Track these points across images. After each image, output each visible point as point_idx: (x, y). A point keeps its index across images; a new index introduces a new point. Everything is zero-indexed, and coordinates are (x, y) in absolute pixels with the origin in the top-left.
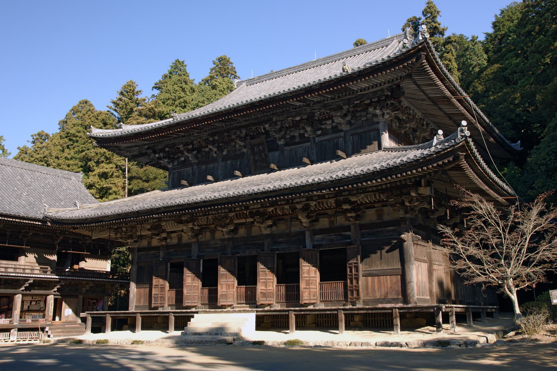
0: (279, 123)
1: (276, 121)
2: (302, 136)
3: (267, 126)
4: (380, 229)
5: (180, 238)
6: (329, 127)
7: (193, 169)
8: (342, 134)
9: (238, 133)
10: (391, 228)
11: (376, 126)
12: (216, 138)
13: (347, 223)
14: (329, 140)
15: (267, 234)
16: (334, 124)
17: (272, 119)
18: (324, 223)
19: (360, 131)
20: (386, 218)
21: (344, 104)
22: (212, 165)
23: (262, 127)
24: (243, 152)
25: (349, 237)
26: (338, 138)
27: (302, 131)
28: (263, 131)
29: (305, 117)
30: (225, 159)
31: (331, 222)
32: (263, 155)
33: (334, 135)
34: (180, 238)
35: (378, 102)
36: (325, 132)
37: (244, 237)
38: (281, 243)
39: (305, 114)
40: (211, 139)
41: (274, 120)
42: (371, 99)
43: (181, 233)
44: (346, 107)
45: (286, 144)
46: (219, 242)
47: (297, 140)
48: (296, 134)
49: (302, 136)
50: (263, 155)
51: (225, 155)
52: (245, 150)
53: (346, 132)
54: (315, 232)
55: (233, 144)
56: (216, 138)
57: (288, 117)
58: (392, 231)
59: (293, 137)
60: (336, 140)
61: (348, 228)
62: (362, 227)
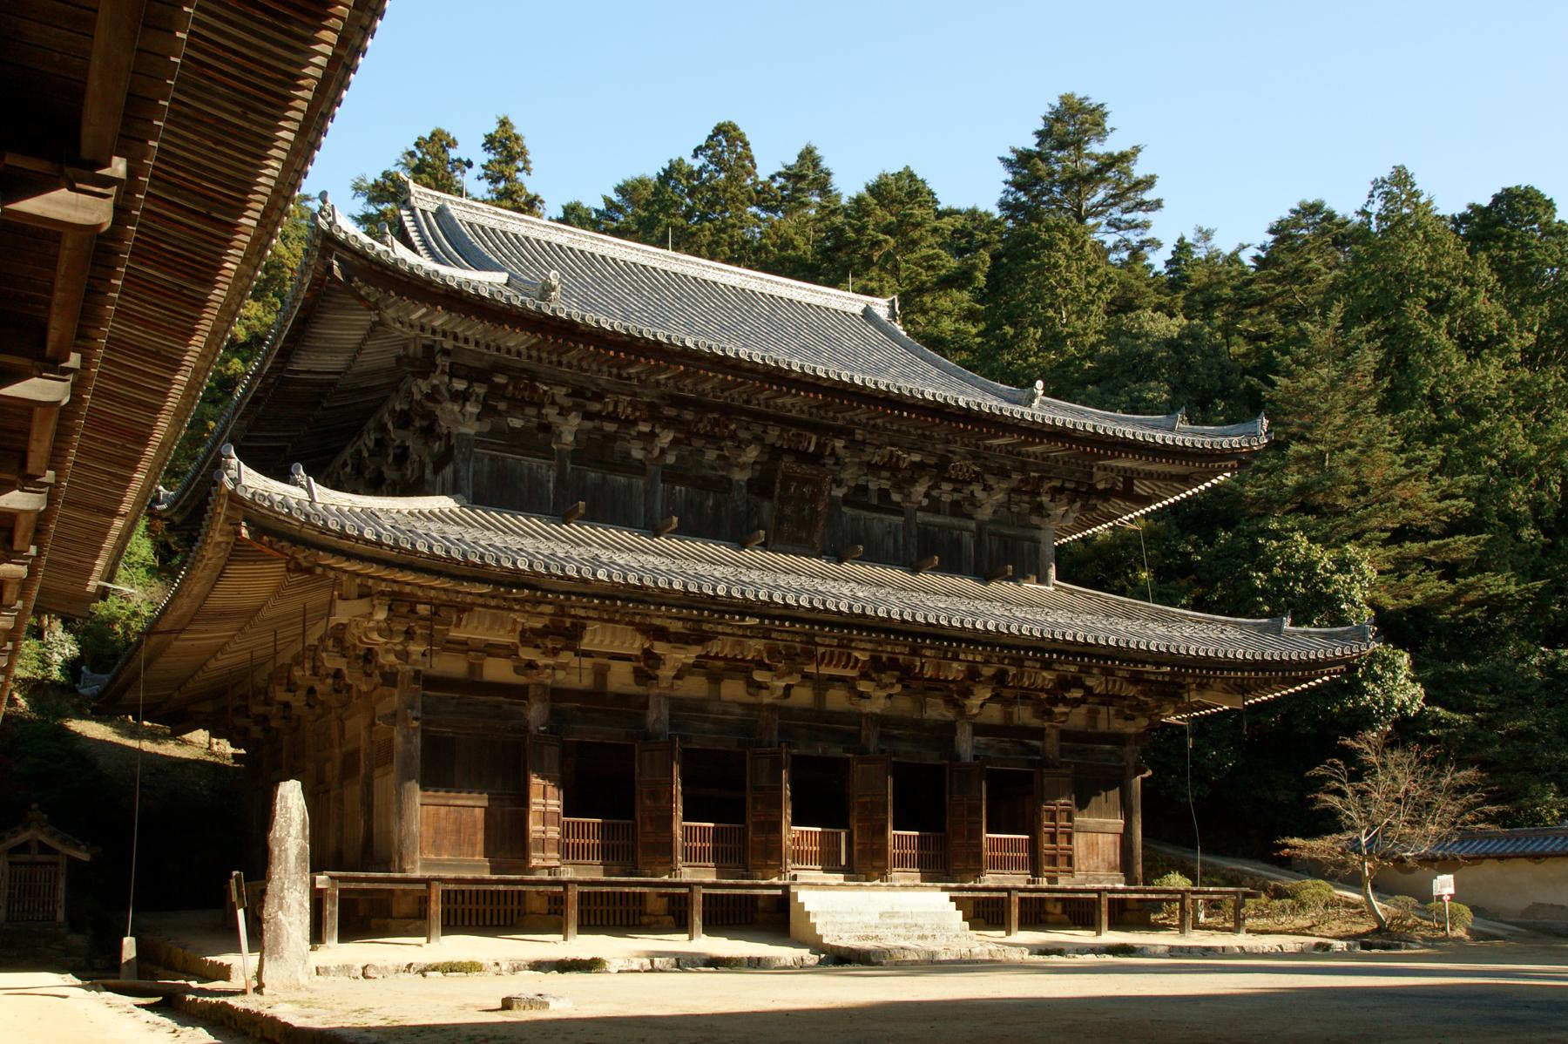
0: (869, 449)
1: (864, 442)
2: (884, 494)
3: (839, 444)
4: (1089, 746)
5: (601, 674)
6: (946, 498)
7: (561, 471)
8: (973, 525)
9: (757, 429)
10: (1108, 747)
11: (1036, 533)
12: (689, 415)
13: (1035, 722)
14: (942, 527)
15: (876, 715)
16: (956, 496)
17: (852, 432)
18: (994, 713)
19: (1005, 531)
20: (1102, 726)
21: (1015, 469)
22: (622, 480)
23: (814, 439)
24: (729, 481)
25: (1036, 751)
26: (961, 529)
27: (885, 484)
28: (812, 449)
29: (932, 461)
30: (671, 475)
31: (1008, 716)
32: (807, 512)
33: (955, 521)
34: (601, 674)
35: (1074, 490)
36: (934, 506)
37: (806, 710)
38: (896, 738)
39: (930, 454)
40: (669, 412)
41: (859, 435)
42: (1064, 481)
43: (605, 661)
44: (1016, 477)
45: (846, 501)
46: (738, 710)
47: (875, 501)
48: (873, 486)
49: (884, 494)
50: (807, 512)
51: (671, 466)
52: (740, 476)
53: (981, 525)
54: (980, 729)
55: (698, 443)
56: (689, 415)
57: (892, 445)
58: (1109, 752)
59: (865, 489)
60: (956, 533)
61: (1039, 733)
62: (1065, 735)
